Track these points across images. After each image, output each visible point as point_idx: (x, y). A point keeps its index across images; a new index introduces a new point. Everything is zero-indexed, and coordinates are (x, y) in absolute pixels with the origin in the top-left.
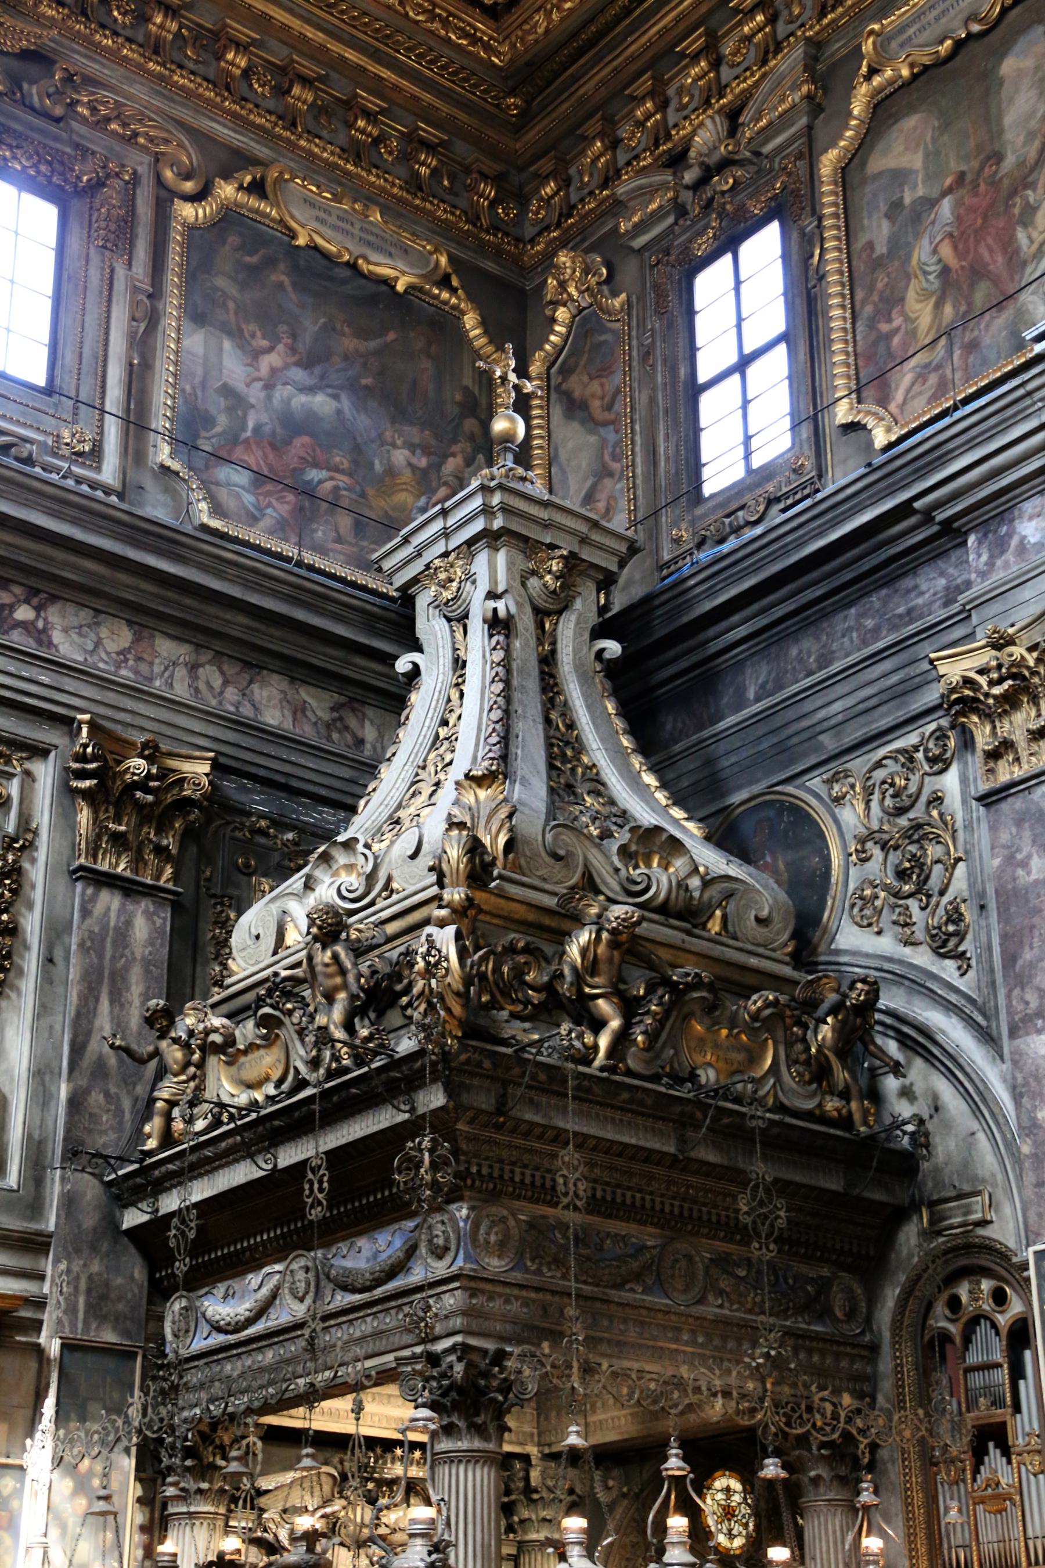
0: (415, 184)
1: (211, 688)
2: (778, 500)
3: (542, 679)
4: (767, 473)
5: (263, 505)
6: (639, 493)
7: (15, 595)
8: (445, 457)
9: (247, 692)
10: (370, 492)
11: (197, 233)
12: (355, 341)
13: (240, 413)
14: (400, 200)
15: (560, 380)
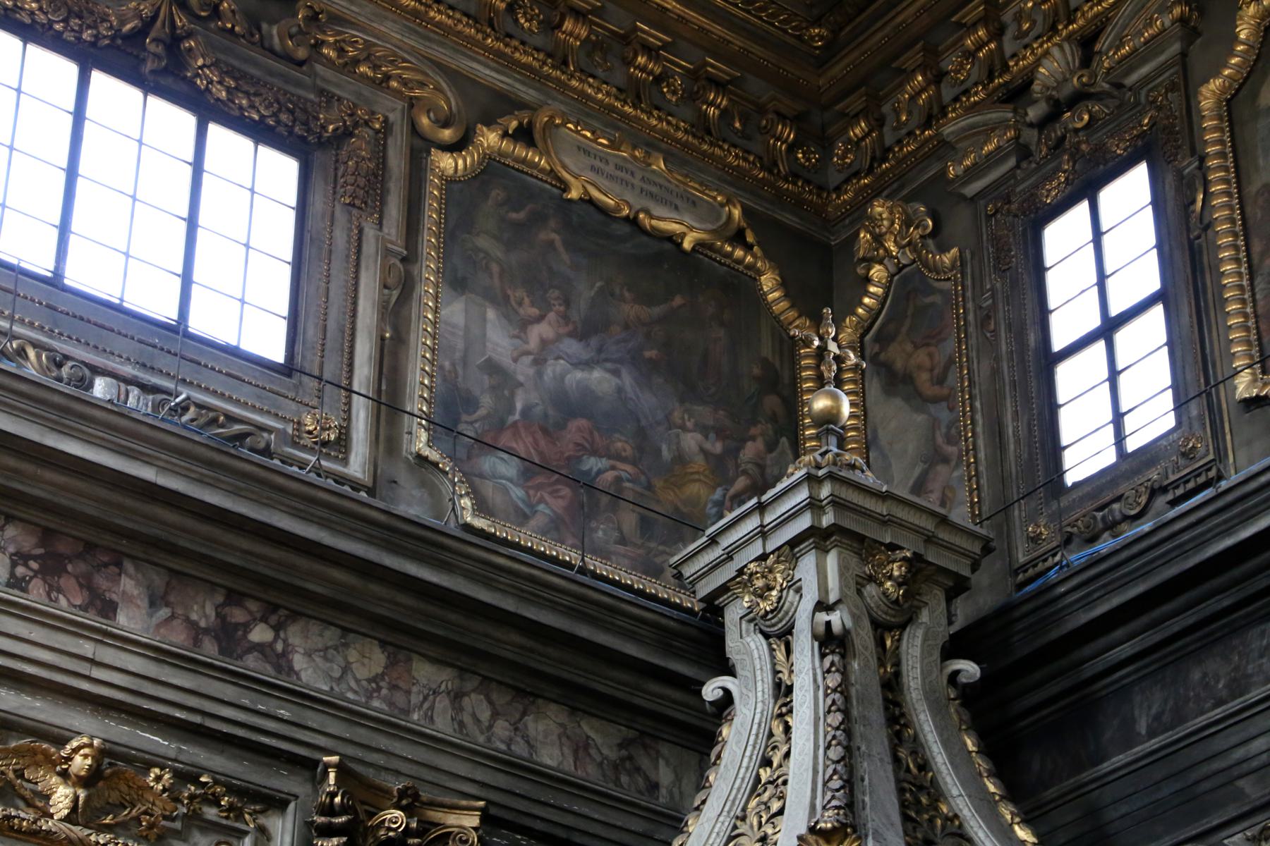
0: (702, 127)
1: (477, 721)
2: (1164, 490)
3: (886, 709)
4: (1149, 454)
5: (534, 500)
6: (984, 481)
7: (250, 613)
8: (744, 441)
9: (520, 726)
10: (658, 483)
11: (456, 187)
12: (636, 306)
13: (506, 392)
14: (685, 145)
15: (877, 348)
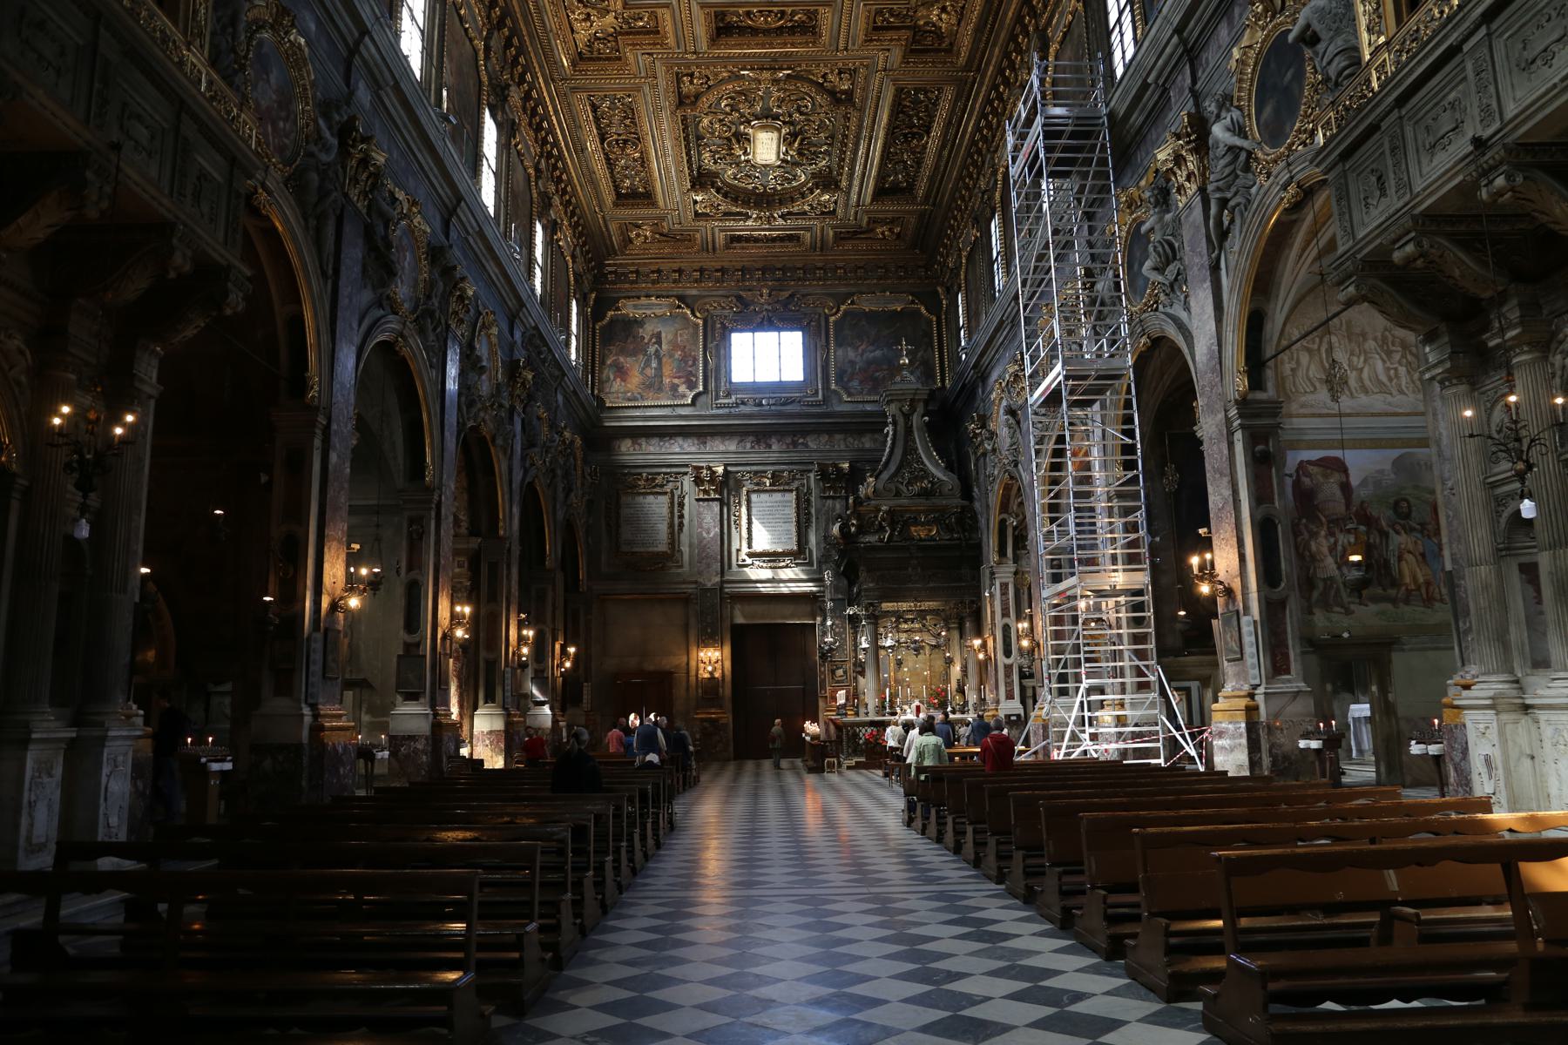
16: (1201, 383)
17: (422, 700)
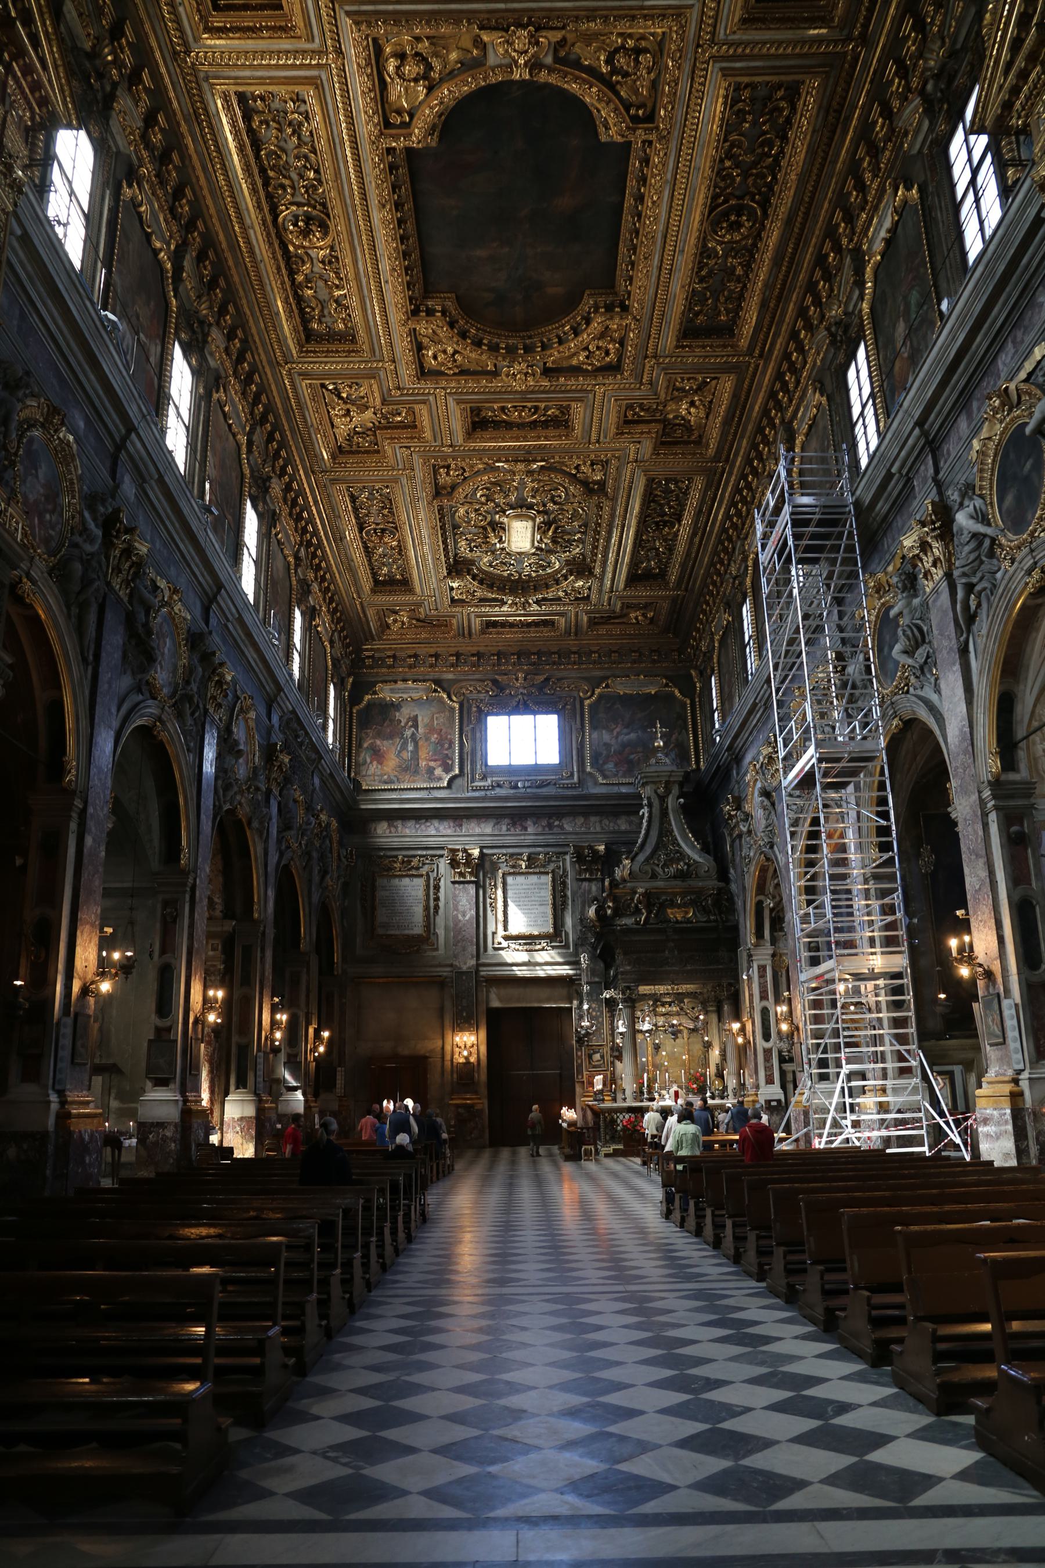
0: (654, 661)
16: (954, 765)
17: (172, 1086)
